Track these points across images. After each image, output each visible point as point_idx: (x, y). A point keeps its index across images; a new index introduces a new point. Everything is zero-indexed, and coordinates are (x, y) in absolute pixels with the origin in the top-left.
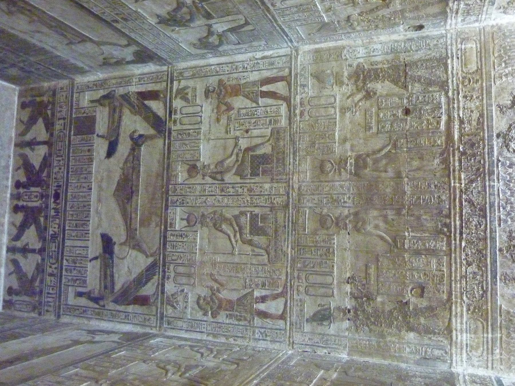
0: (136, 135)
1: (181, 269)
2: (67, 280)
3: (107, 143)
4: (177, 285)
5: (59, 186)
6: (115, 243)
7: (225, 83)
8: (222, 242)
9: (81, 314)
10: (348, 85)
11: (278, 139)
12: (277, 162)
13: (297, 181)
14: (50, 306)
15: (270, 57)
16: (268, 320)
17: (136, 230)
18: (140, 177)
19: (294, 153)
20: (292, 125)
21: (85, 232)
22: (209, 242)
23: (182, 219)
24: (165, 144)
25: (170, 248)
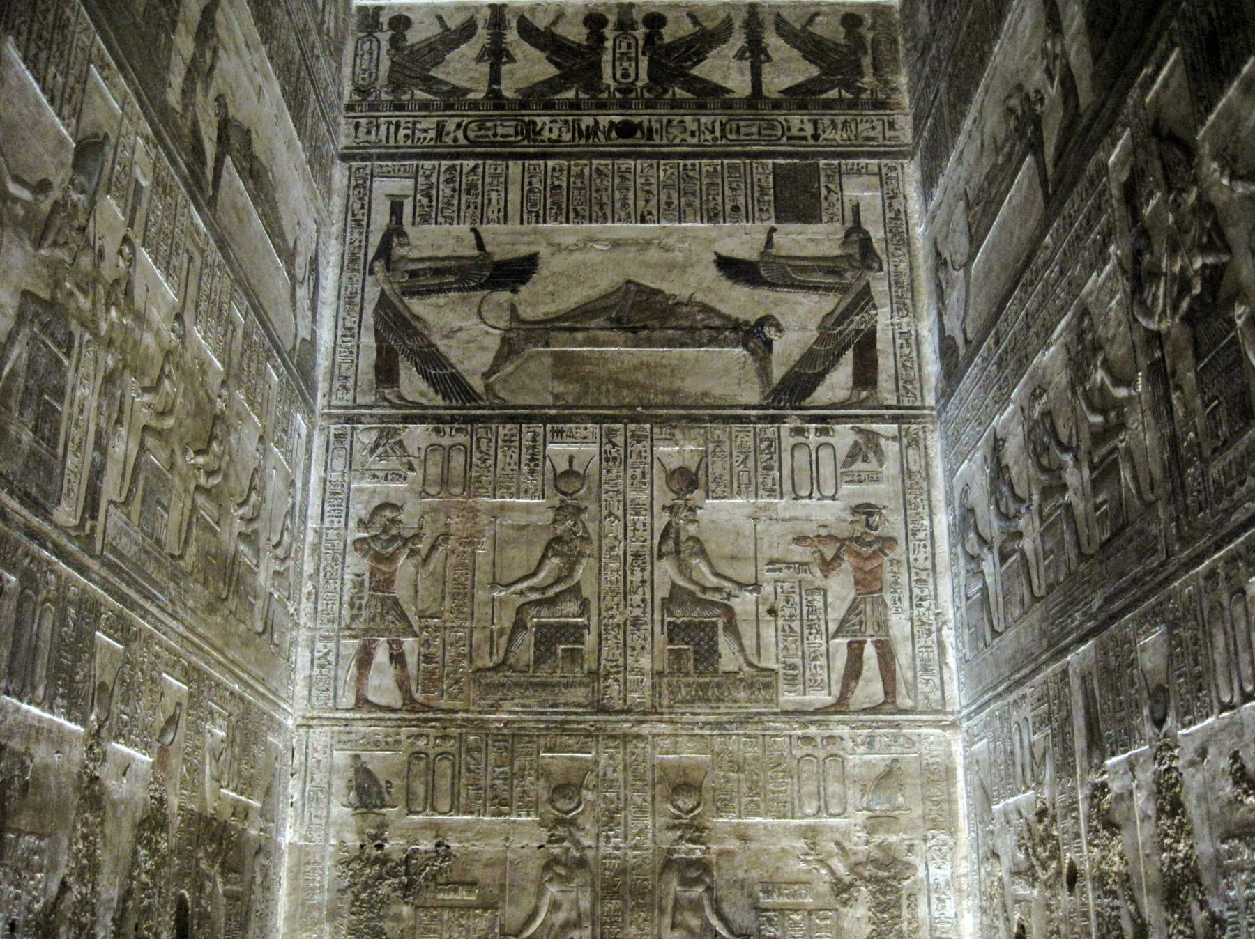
0: (770, 332)
1: (458, 460)
2: (428, 173)
3: (754, 256)
4: (423, 453)
5: (650, 134)
6: (515, 291)
7: (886, 555)
8: (520, 558)
9: (354, 215)
10: (867, 843)
11: (751, 685)
12: (699, 685)
13: (655, 731)
14: (369, 132)
15: (942, 663)
16: (353, 670)
17: (547, 345)
18: (670, 346)
19: (718, 724)
20: (784, 718)
21: (541, 212)
22: (523, 528)
23: (571, 459)
24: (746, 407)
25: (506, 431)
